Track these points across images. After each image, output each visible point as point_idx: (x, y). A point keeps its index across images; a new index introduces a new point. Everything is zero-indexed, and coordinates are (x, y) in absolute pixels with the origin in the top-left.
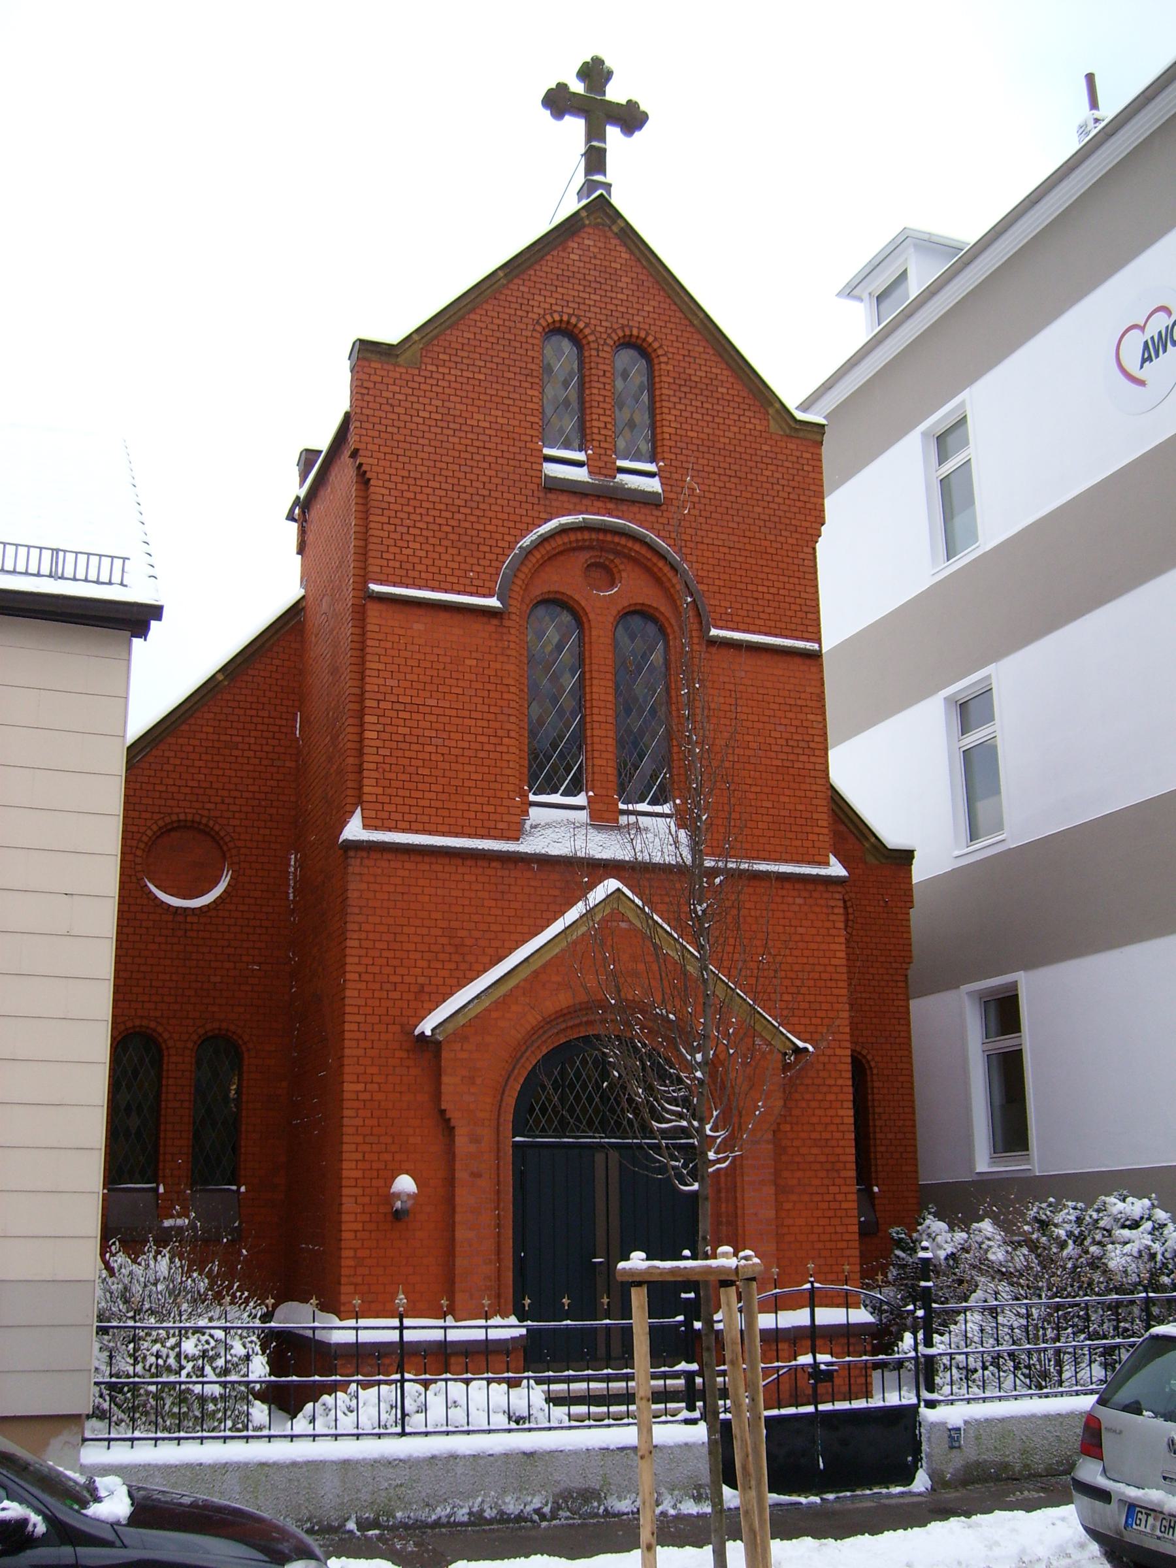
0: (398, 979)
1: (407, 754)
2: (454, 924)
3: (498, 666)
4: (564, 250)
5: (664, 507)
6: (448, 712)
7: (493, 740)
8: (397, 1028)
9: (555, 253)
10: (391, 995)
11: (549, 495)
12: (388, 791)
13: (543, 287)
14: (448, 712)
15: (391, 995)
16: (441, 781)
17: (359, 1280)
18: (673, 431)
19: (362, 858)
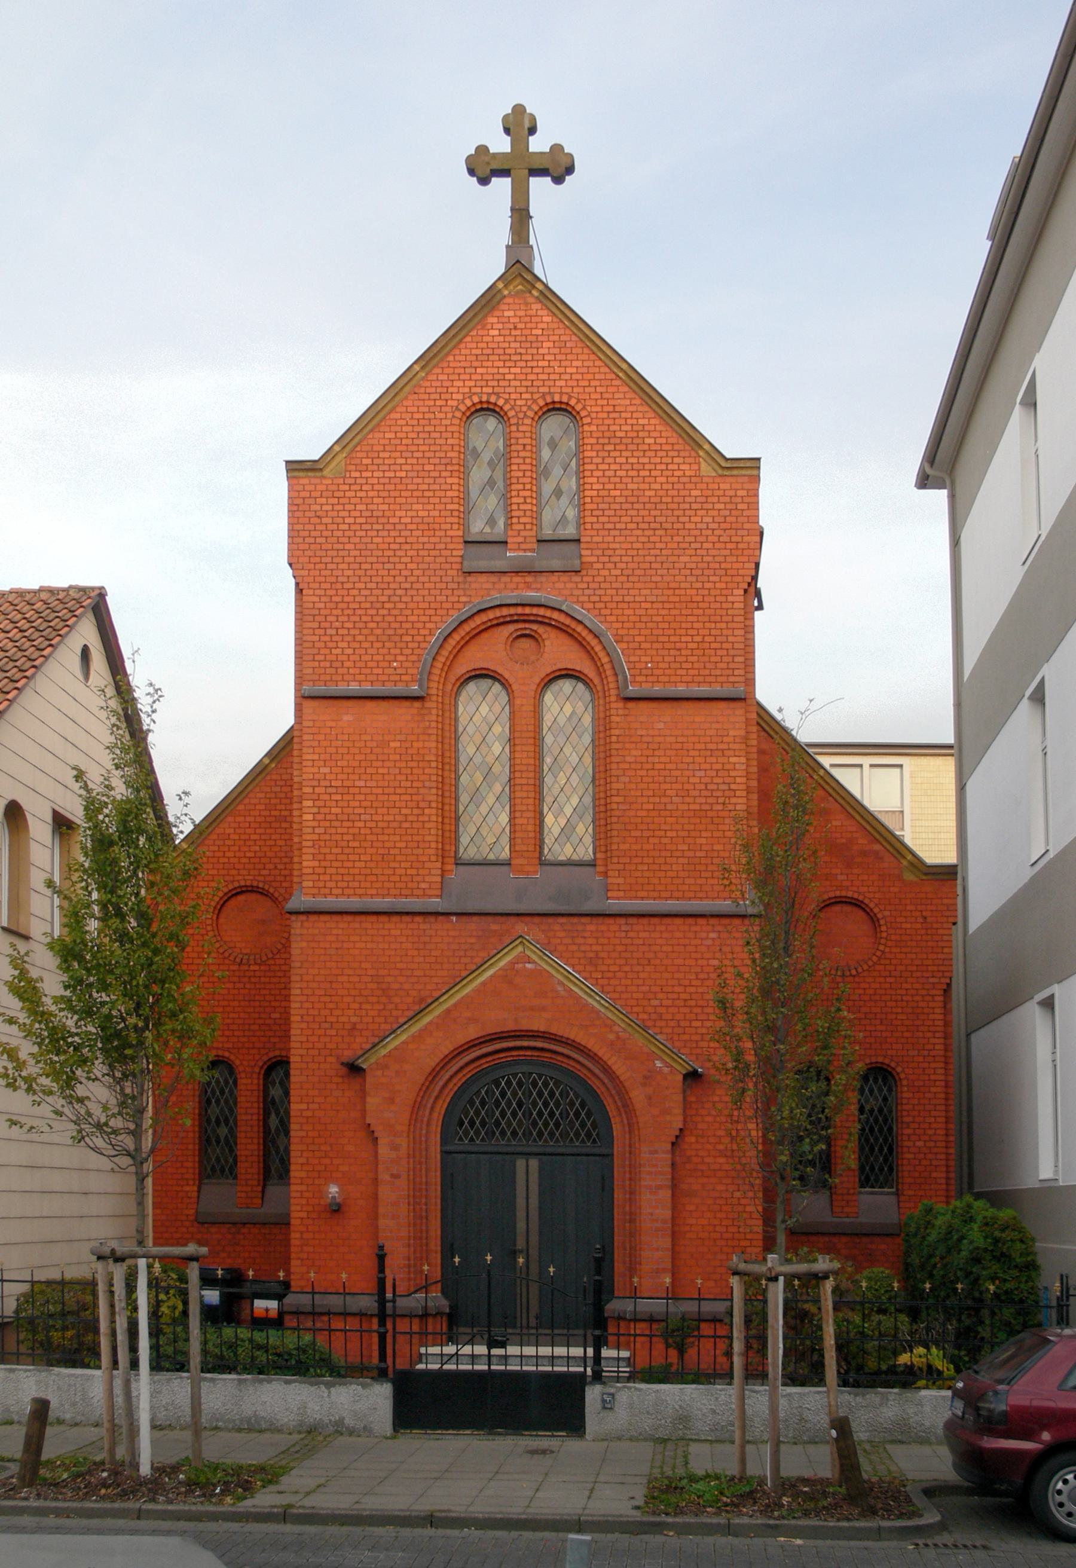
0: (334, 1019)
1: (339, 830)
2: (382, 972)
3: (421, 744)
4: (482, 329)
5: (584, 572)
6: (375, 791)
7: (415, 811)
8: (332, 1059)
9: (474, 333)
10: (329, 1032)
11: (469, 579)
12: (323, 864)
13: (462, 371)
14: (375, 791)
15: (329, 1032)
16: (370, 851)
17: (305, 1256)
18: (595, 493)
19: (302, 922)
